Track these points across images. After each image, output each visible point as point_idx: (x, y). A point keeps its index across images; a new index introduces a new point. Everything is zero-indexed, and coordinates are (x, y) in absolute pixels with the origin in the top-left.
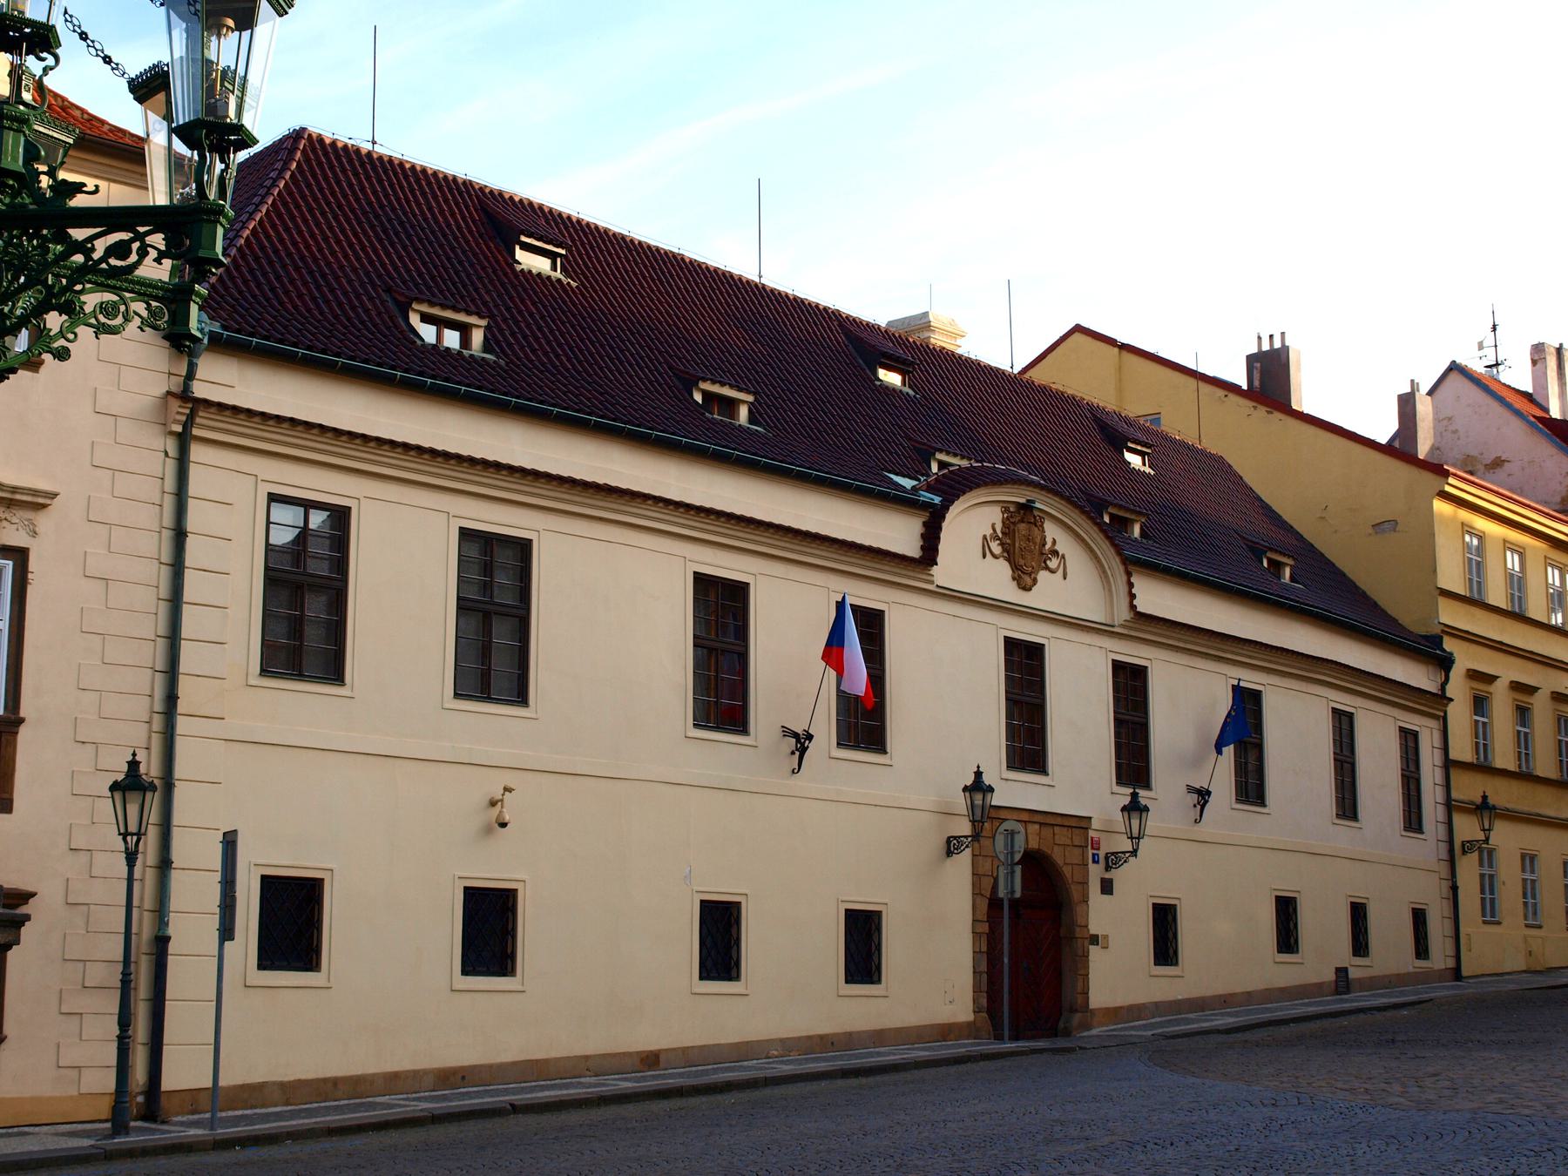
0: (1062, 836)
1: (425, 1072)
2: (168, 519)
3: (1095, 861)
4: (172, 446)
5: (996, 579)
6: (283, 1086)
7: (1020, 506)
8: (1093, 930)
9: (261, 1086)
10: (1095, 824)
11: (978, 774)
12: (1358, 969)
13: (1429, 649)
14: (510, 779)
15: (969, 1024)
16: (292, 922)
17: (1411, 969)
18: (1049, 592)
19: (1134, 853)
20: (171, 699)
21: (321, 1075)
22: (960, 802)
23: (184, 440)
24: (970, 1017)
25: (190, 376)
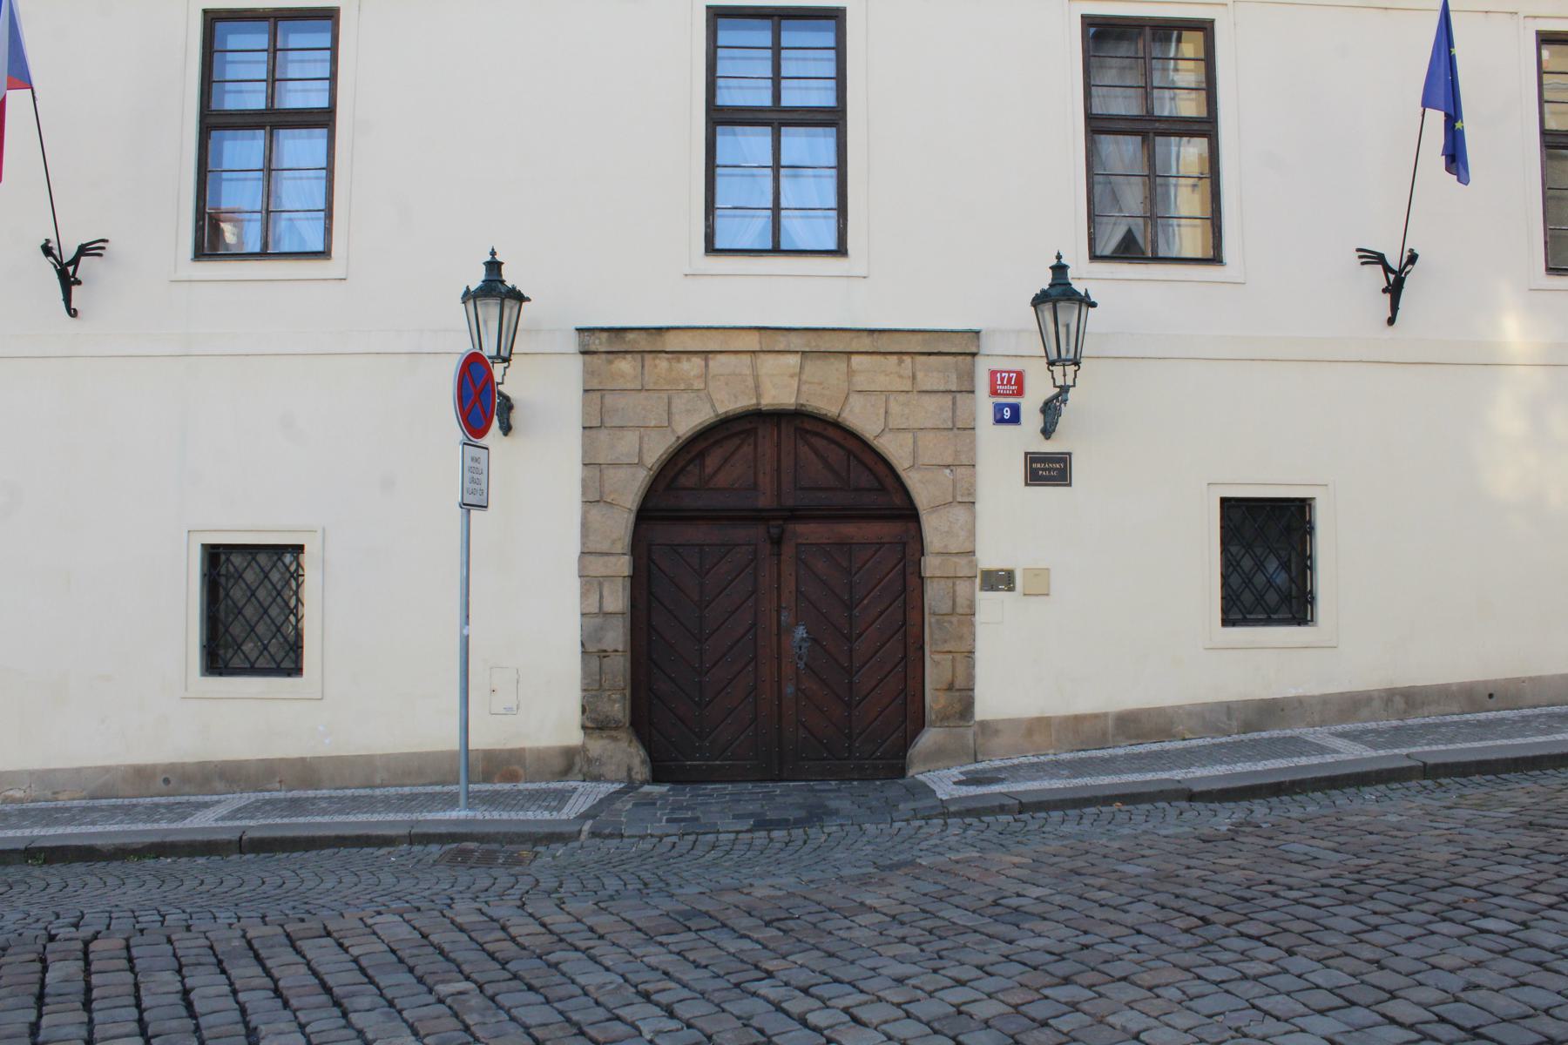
8: (989, 558)
10: (987, 346)
11: (494, 266)
15: (569, 754)
19: (1064, 389)
24: (575, 737)
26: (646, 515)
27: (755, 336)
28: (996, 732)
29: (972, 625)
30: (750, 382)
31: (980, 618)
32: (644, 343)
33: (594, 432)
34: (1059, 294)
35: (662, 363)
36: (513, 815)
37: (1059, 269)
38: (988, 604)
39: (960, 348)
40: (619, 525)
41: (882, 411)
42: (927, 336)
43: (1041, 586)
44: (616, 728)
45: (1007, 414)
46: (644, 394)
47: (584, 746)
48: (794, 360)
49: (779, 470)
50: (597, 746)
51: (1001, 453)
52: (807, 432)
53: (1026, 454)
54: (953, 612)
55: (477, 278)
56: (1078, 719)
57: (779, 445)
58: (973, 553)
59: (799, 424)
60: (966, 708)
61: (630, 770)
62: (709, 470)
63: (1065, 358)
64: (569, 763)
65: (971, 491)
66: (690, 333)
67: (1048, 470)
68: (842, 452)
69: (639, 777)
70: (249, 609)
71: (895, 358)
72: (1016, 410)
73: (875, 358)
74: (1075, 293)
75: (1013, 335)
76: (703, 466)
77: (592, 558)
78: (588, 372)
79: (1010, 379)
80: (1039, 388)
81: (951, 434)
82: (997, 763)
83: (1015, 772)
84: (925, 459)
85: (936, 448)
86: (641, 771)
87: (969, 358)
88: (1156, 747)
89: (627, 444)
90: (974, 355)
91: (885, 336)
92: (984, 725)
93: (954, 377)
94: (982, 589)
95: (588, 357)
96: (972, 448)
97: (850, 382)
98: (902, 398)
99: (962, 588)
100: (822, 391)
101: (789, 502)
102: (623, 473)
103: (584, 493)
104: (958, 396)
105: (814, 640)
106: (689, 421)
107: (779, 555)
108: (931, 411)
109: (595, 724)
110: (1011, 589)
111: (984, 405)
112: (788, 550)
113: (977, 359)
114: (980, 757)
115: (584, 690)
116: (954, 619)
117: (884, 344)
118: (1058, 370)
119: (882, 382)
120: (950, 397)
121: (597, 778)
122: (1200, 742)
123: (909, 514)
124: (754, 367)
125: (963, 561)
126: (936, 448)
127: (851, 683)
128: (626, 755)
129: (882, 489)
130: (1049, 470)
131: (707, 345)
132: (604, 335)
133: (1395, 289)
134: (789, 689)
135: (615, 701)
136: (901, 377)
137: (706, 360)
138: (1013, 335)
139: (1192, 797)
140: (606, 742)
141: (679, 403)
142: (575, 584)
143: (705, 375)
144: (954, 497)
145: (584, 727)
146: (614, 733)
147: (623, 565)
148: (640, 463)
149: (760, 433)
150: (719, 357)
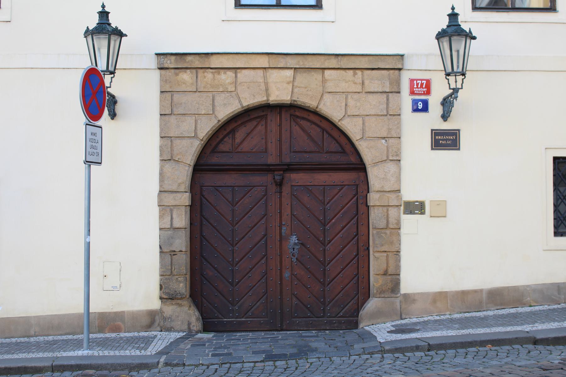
8: (409, 194)
10: (408, 64)
11: (104, 14)
19: (456, 91)
24: (155, 304)
26: (200, 168)
27: (266, 58)
28: (414, 301)
29: (399, 235)
30: (263, 87)
31: (403, 231)
32: (197, 63)
33: (167, 117)
35: (209, 75)
36: (117, 353)
37: (453, 16)
39: (393, 65)
40: (183, 175)
41: (344, 104)
42: (371, 58)
43: (441, 212)
44: (181, 299)
45: (420, 106)
46: (197, 94)
47: (161, 309)
48: (290, 73)
49: (280, 141)
50: (170, 309)
51: (416, 131)
52: (298, 117)
53: (432, 130)
54: (387, 227)
55: (93, 22)
56: (464, 293)
57: (280, 125)
58: (399, 191)
59: (292, 111)
60: (395, 286)
61: (189, 324)
62: (238, 140)
63: (456, 71)
64: (152, 320)
65: (398, 153)
66: (226, 57)
67: (445, 140)
68: (319, 130)
69: (195, 328)
71: (351, 71)
72: (426, 104)
73: (339, 71)
74: (463, 30)
75: (424, 57)
76: (234, 138)
77: (166, 194)
78: (163, 81)
79: (422, 84)
80: (440, 90)
81: (385, 118)
82: (415, 320)
83: (425, 325)
84: (369, 134)
85: (376, 127)
86: (197, 325)
87: (397, 72)
88: (513, 311)
89: (186, 126)
90: (400, 69)
91: (345, 58)
92: (406, 296)
93: (387, 84)
94: (404, 213)
95: (163, 72)
96: (399, 126)
97: (323, 87)
98: (356, 96)
99: (393, 212)
100: (305, 91)
101: (287, 160)
102: (185, 142)
103: (161, 155)
104: (390, 95)
105: (302, 244)
106: (227, 109)
107: (281, 193)
108: (374, 104)
109: (168, 296)
110: (423, 213)
111: (406, 100)
112: (286, 189)
113: (402, 72)
114: (404, 316)
115: (161, 275)
116: (388, 232)
117: (344, 63)
118: (452, 78)
119: (343, 86)
120: (385, 95)
121: (170, 330)
122: (541, 308)
123: (360, 167)
124: (265, 77)
125: (393, 196)
126: (376, 127)
127: (325, 270)
128: (187, 315)
129: (344, 152)
130: (446, 140)
131: (236, 63)
132: (173, 58)
134: (287, 274)
135: (180, 282)
136: (355, 83)
137: (236, 73)
138: (424, 57)
139: (536, 342)
140: (175, 307)
141: (219, 99)
142: (156, 210)
143: (235, 83)
144: (388, 157)
145: (161, 298)
146: (180, 302)
147: (185, 199)
148: (196, 137)
149: (269, 117)
150: (244, 71)
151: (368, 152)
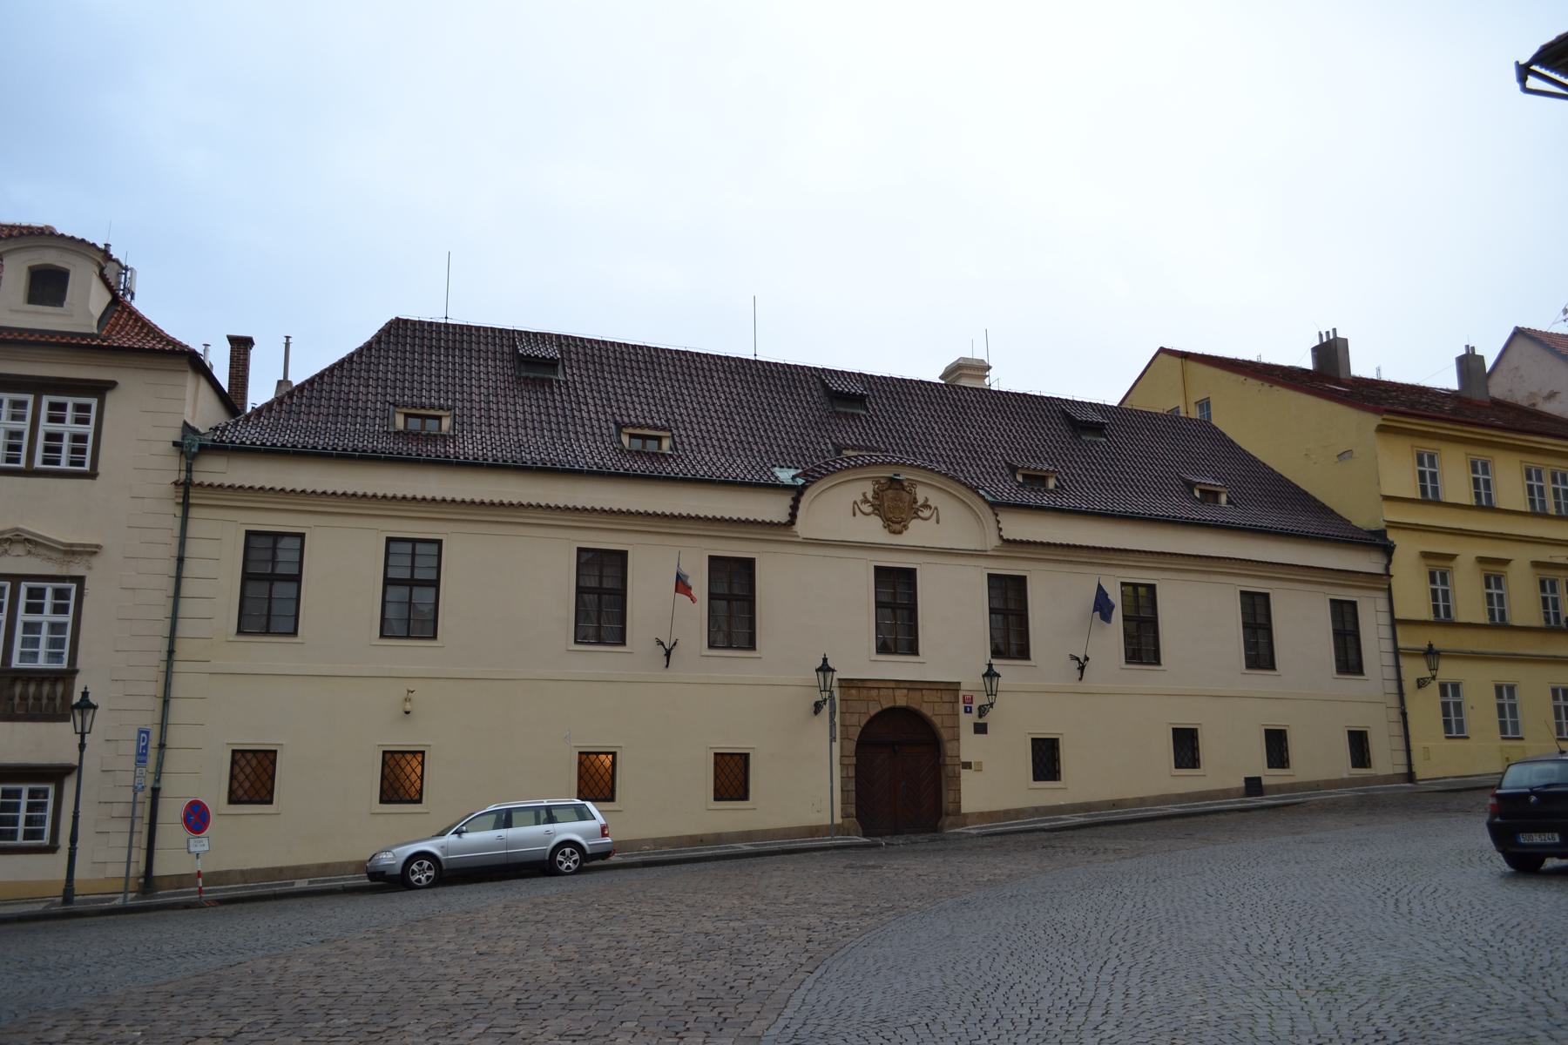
0: (930, 696)
1: (350, 863)
2: (175, 552)
3: (968, 711)
4: (179, 511)
5: (872, 529)
6: (242, 872)
7: (891, 480)
8: (964, 759)
9: (228, 872)
10: (963, 687)
11: (825, 660)
12: (1271, 777)
13: (1377, 541)
14: (412, 685)
16: (253, 776)
17: (1345, 776)
18: (918, 532)
19: (991, 705)
20: (171, 652)
21: (270, 865)
22: (813, 677)
23: (186, 506)
25: (189, 470)
26: (859, 744)
34: (990, 674)
37: (990, 665)
38: (965, 773)
39: (953, 687)
51: (967, 721)
63: (992, 693)
67: (980, 729)
70: (732, 777)
89: (854, 719)
108: (947, 708)
109: (845, 816)
111: (962, 706)
133: (1082, 668)
147: (854, 760)
151: (945, 734)
